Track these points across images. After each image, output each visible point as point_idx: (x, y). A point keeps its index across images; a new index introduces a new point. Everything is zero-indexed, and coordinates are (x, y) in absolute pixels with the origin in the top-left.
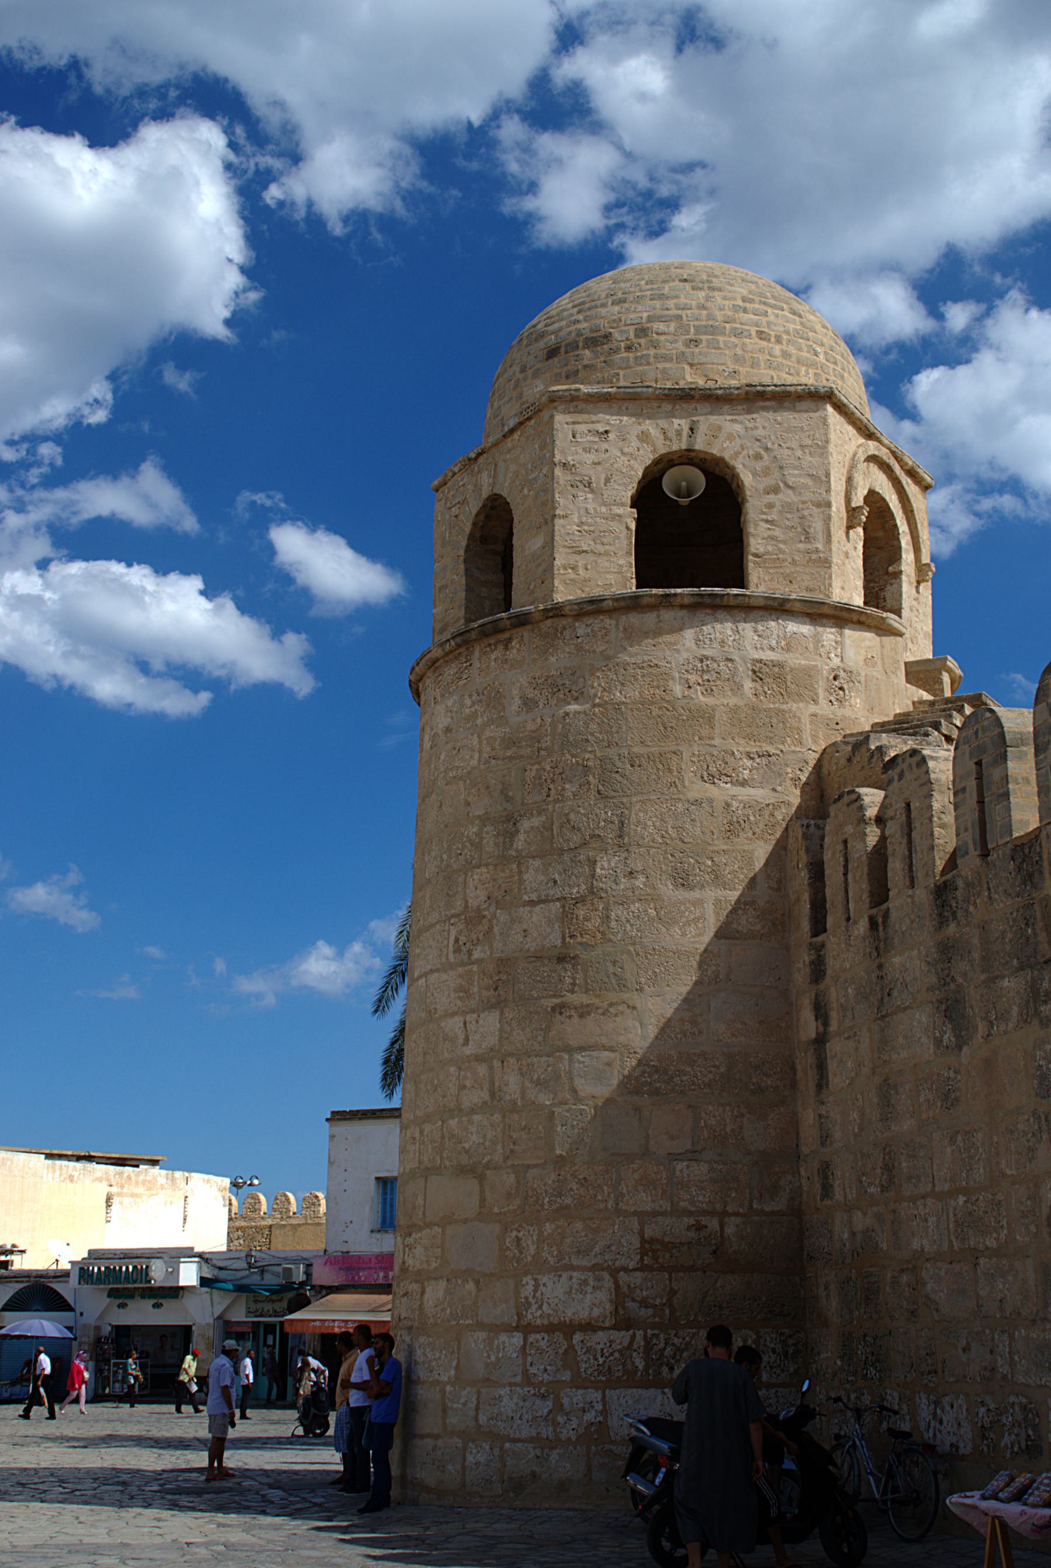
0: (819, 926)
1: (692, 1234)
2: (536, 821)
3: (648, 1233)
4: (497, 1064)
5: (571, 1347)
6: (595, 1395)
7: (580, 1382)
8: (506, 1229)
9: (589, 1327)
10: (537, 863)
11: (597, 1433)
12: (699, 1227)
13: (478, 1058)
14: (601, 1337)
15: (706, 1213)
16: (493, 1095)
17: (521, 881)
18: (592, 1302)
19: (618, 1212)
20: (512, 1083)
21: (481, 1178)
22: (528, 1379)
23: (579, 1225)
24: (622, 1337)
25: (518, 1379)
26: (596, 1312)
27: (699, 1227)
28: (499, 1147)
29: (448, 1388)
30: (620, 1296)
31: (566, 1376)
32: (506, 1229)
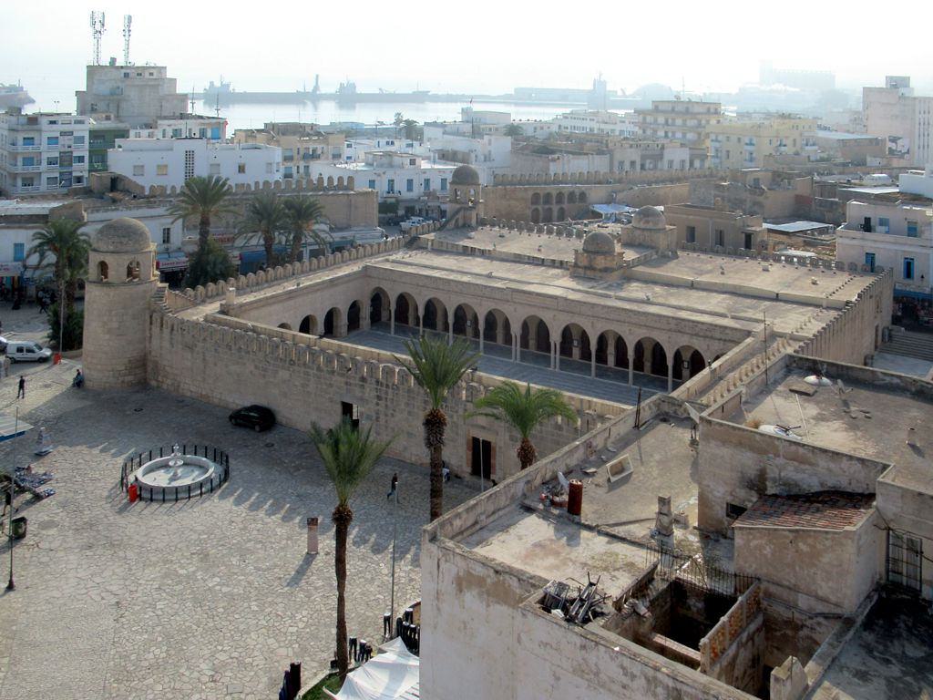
0: (151, 323)
11: (123, 382)
18: (123, 368)
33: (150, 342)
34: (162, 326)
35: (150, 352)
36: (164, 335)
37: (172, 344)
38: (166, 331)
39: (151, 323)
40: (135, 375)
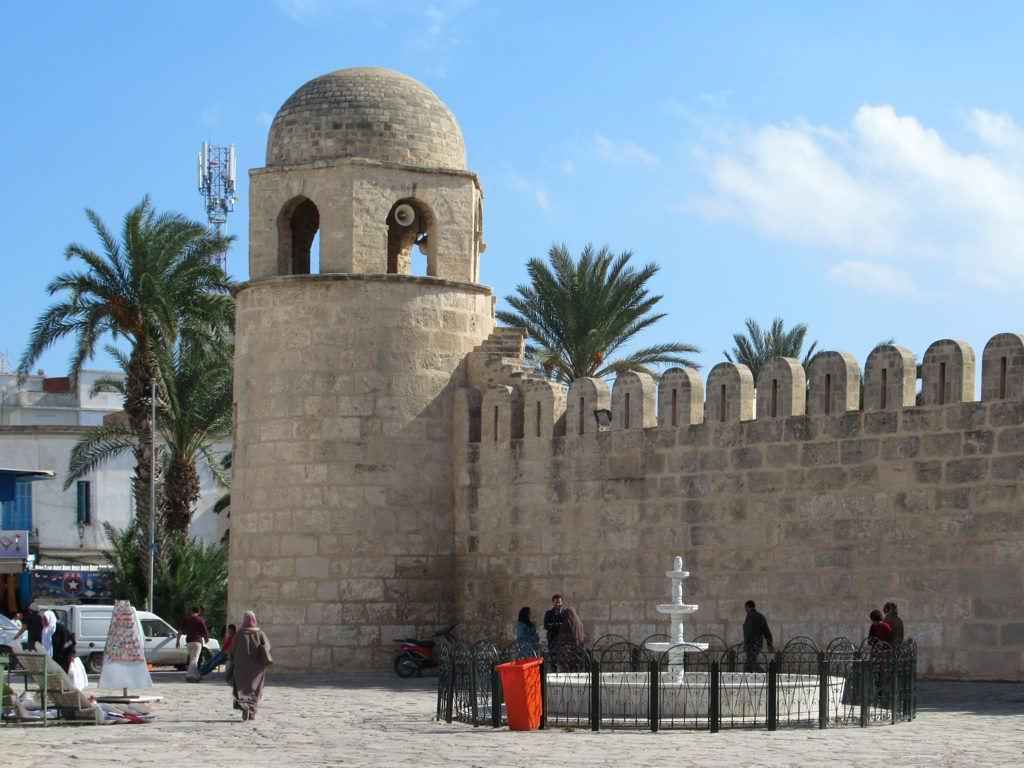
1: (416, 565)
2: (346, 378)
3: (398, 563)
4: (325, 488)
5: (365, 608)
6: (376, 628)
7: (368, 623)
8: (332, 560)
9: (373, 601)
10: (347, 398)
11: (377, 644)
12: (418, 561)
13: (314, 485)
14: (378, 606)
15: (420, 556)
16: (324, 503)
17: (338, 406)
18: (376, 592)
19: (387, 555)
20: (335, 498)
21: (318, 538)
22: (344, 622)
23: (368, 560)
24: (387, 606)
25: (340, 622)
26: (376, 595)
27: (418, 561)
28: (328, 525)
29: (300, 627)
30: (386, 589)
31: (363, 621)
32: (332, 560)
33: (473, 503)
34: (518, 433)
35: (473, 542)
36: (525, 464)
37: (559, 488)
38: (536, 445)
39: (475, 435)
40: (418, 623)
